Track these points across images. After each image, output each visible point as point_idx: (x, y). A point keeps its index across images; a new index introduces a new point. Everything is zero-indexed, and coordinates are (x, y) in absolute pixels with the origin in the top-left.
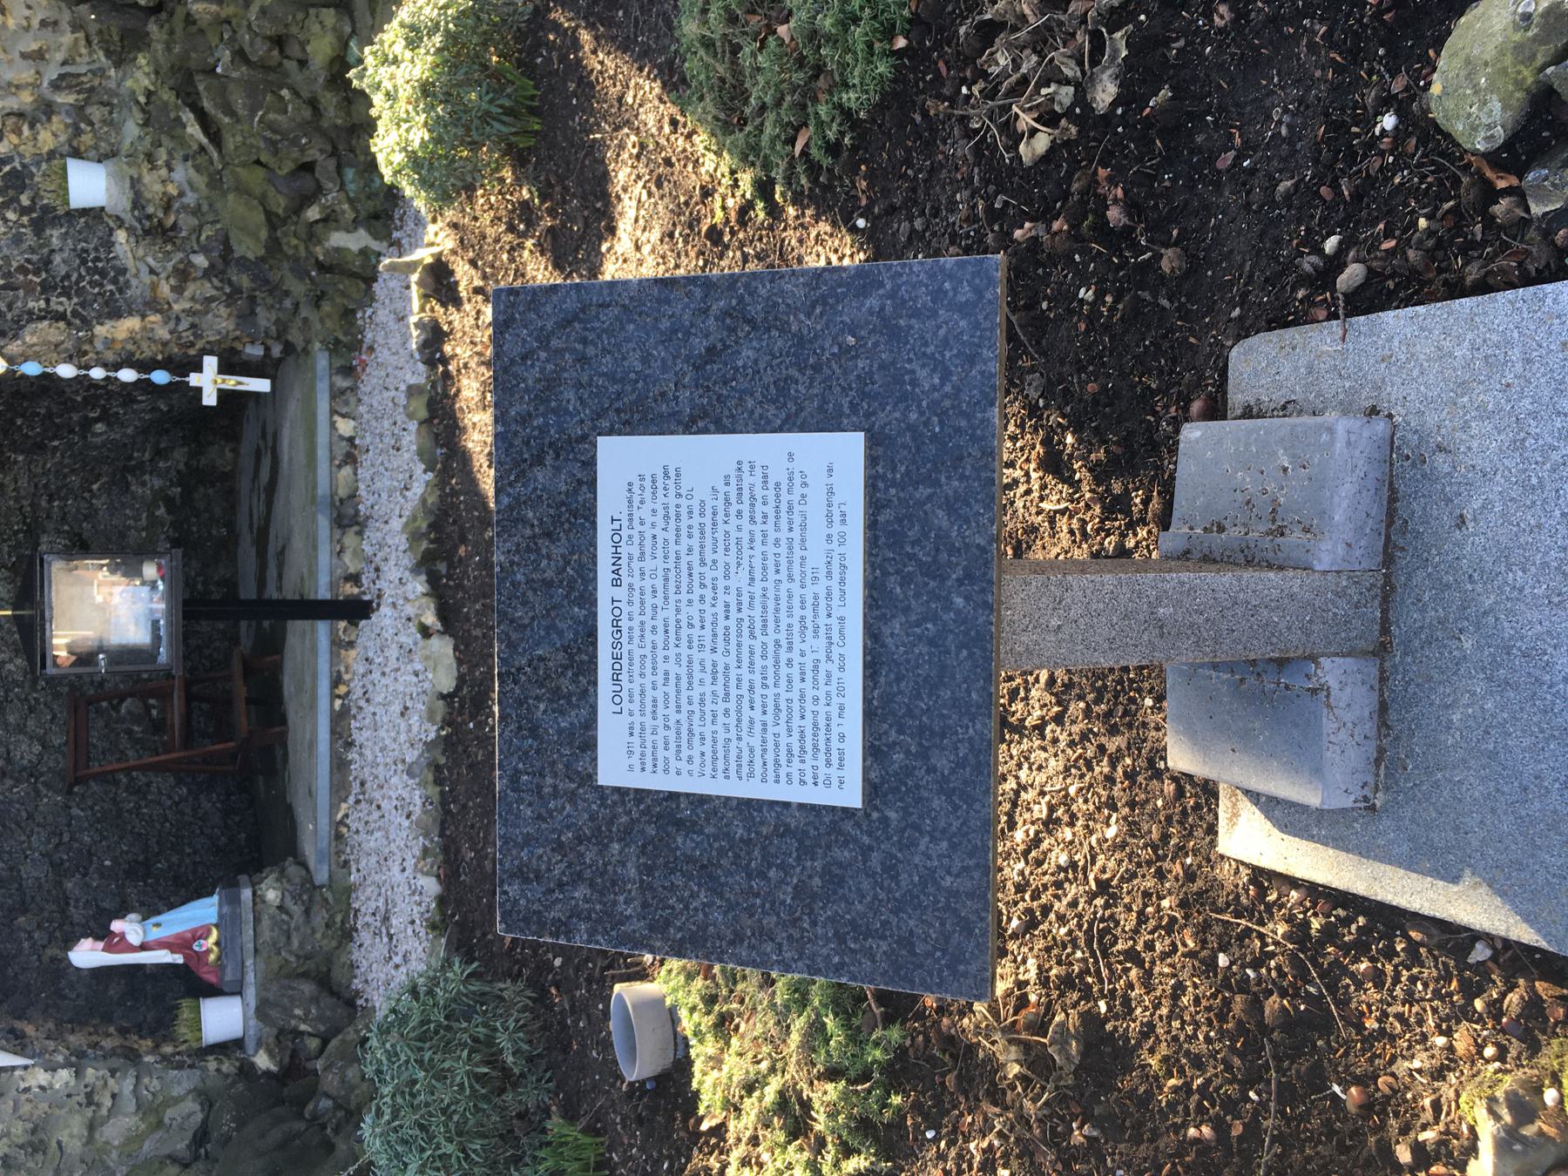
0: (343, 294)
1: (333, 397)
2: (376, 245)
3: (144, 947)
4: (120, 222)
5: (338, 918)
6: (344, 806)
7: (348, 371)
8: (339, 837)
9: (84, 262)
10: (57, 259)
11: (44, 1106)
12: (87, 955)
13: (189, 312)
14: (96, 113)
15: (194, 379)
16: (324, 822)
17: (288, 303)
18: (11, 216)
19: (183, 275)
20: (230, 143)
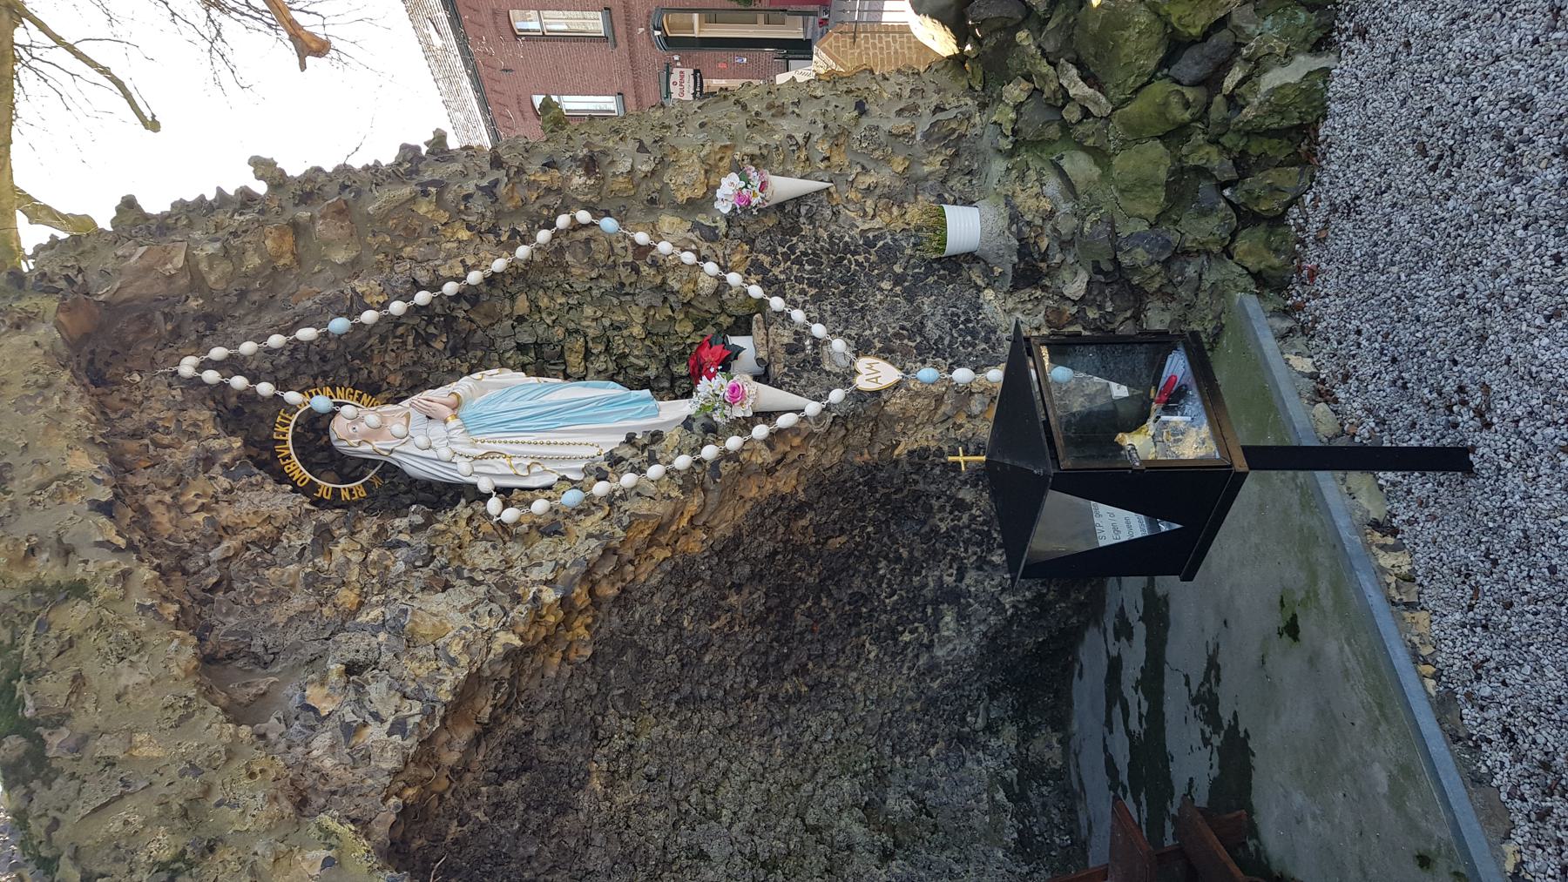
6: (1509, 848)
9: (955, 325)
10: (930, 324)
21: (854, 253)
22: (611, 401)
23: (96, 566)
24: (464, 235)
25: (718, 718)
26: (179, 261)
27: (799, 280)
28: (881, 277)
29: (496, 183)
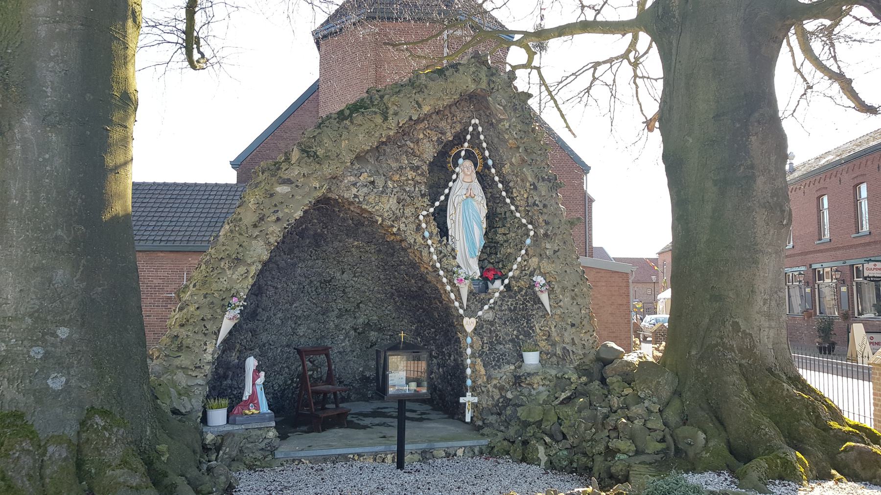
0: (515, 451)
1: (470, 447)
2: (543, 463)
3: (254, 384)
4: (520, 367)
5: (258, 463)
7: (481, 453)
8: (294, 461)
10: (502, 346)
11: (197, 350)
12: (251, 363)
13: (488, 391)
14: (554, 359)
15: (469, 394)
16: (303, 454)
17: (502, 428)
18: (515, 332)
19: (501, 389)
20: (567, 410)
22: (474, 244)
23: (392, 122)
24: (525, 196)
25: (382, 277)
26: (502, 117)
27: (517, 304)
28: (518, 331)
29: (537, 206)
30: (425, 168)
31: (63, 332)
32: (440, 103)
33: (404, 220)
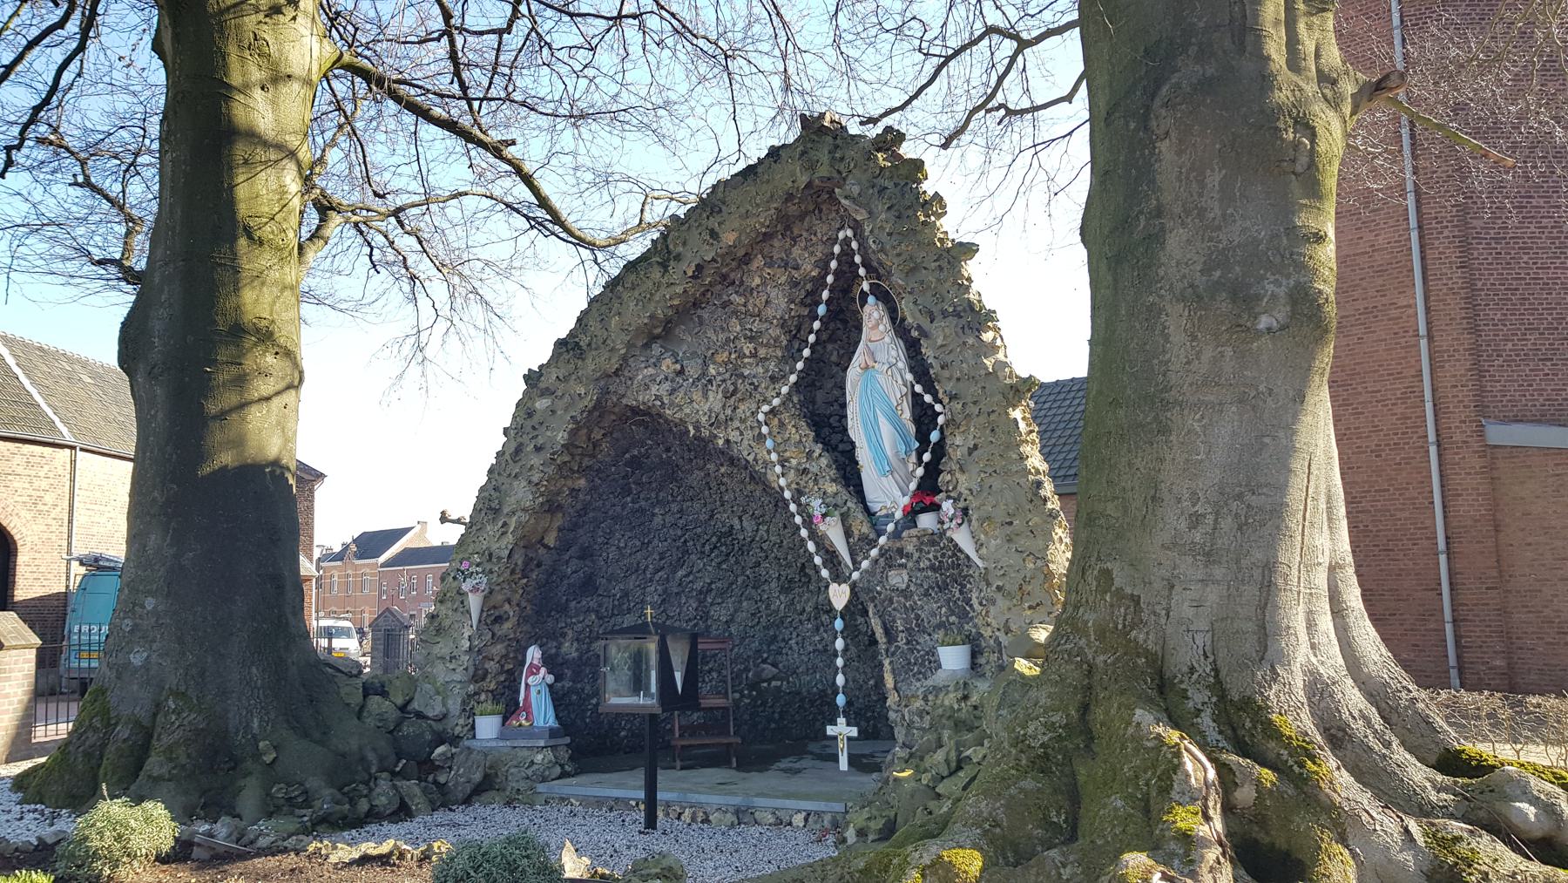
12: (534, 654)
15: (841, 720)
21: (961, 592)
27: (943, 555)
30: (775, 332)
31: (150, 603)
32: (751, 221)
33: (737, 424)
